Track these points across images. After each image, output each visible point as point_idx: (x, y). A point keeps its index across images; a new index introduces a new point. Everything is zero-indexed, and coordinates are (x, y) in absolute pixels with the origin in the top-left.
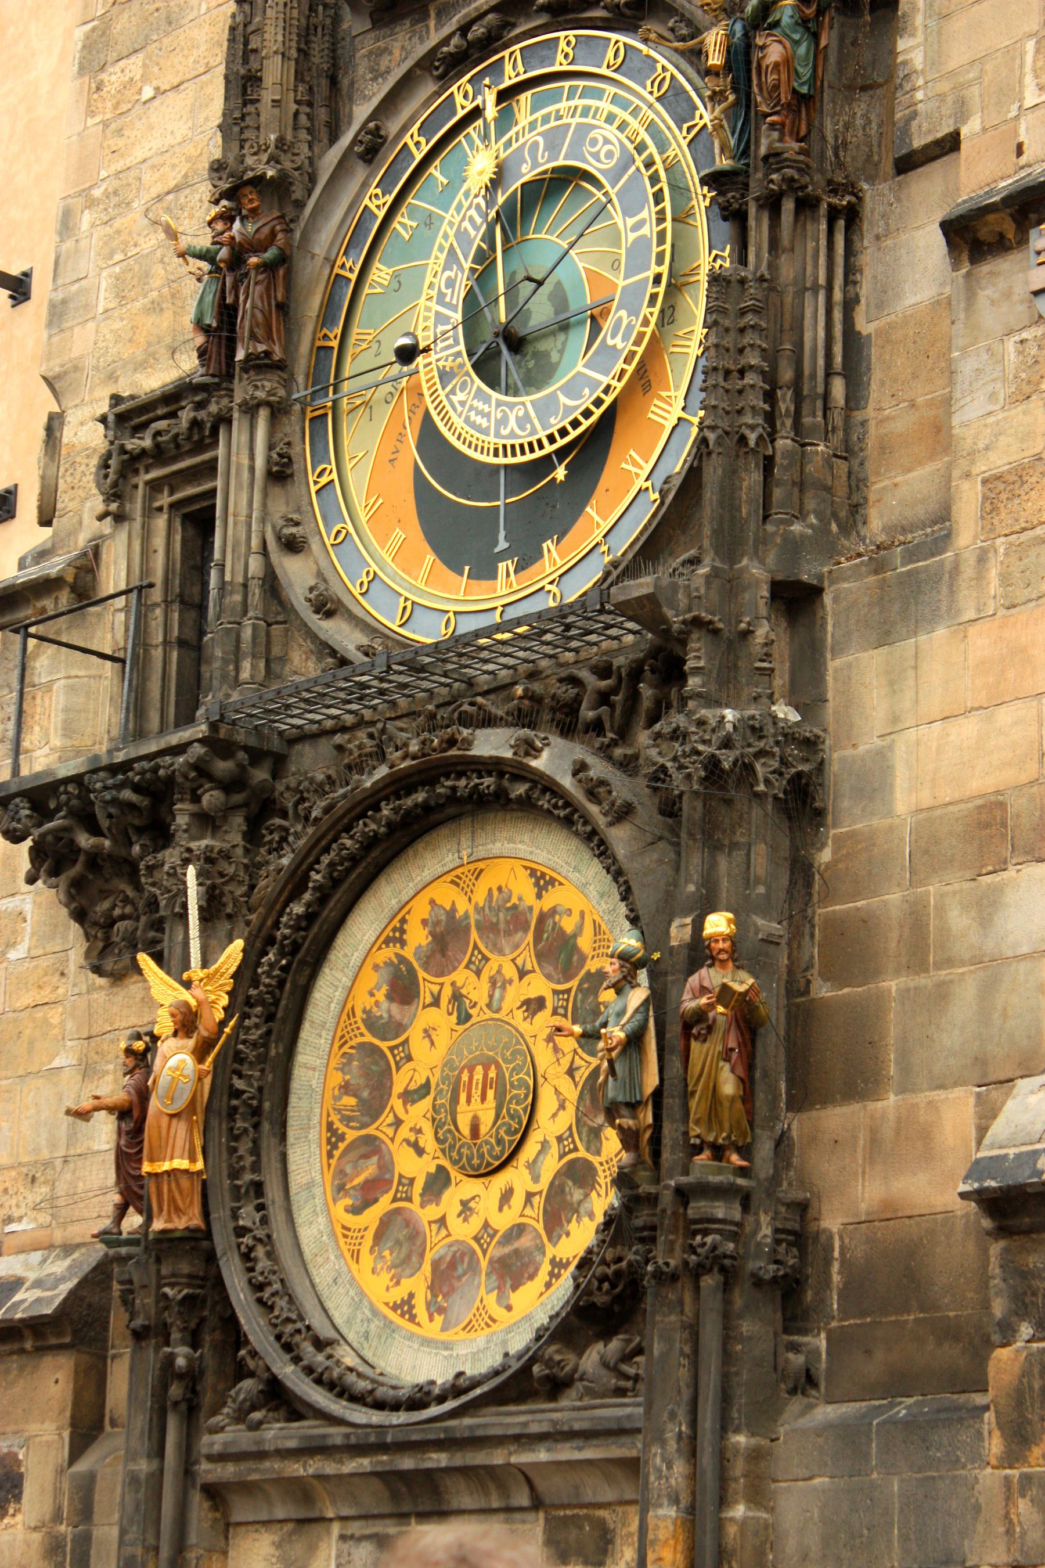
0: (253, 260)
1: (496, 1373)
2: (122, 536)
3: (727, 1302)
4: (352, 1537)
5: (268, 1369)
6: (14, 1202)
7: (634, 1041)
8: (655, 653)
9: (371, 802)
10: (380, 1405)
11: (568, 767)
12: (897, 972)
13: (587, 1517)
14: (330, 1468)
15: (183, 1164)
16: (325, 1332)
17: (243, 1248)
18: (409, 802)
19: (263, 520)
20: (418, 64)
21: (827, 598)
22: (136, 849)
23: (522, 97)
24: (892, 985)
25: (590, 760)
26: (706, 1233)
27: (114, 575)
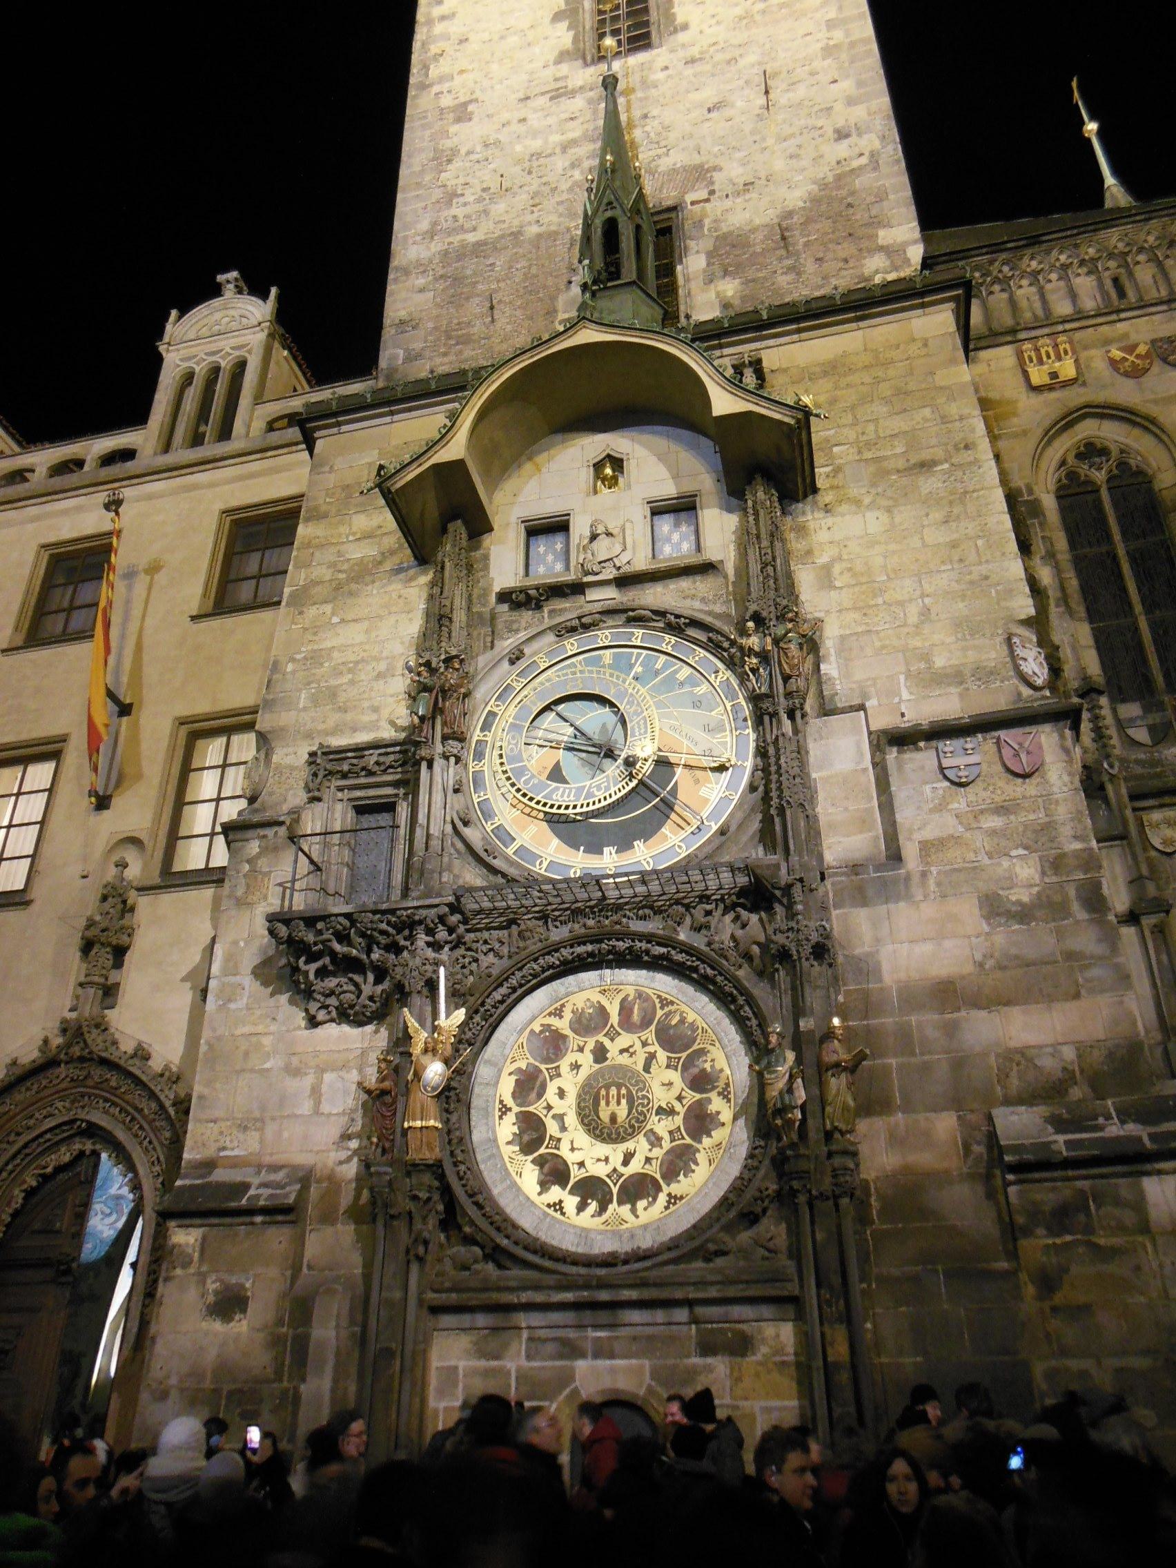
1: (669, 1249)
2: (318, 807)
4: (539, 1339)
5: (492, 1240)
6: (228, 1139)
8: (743, 892)
10: (575, 1263)
12: (895, 1056)
13: (729, 1329)
17: (462, 1173)
18: (580, 950)
19: (452, 808)
20: (549, 628)
22: (375, 956)
23: (608, 652)
24: (893, 1062)
26: (843, 1175)
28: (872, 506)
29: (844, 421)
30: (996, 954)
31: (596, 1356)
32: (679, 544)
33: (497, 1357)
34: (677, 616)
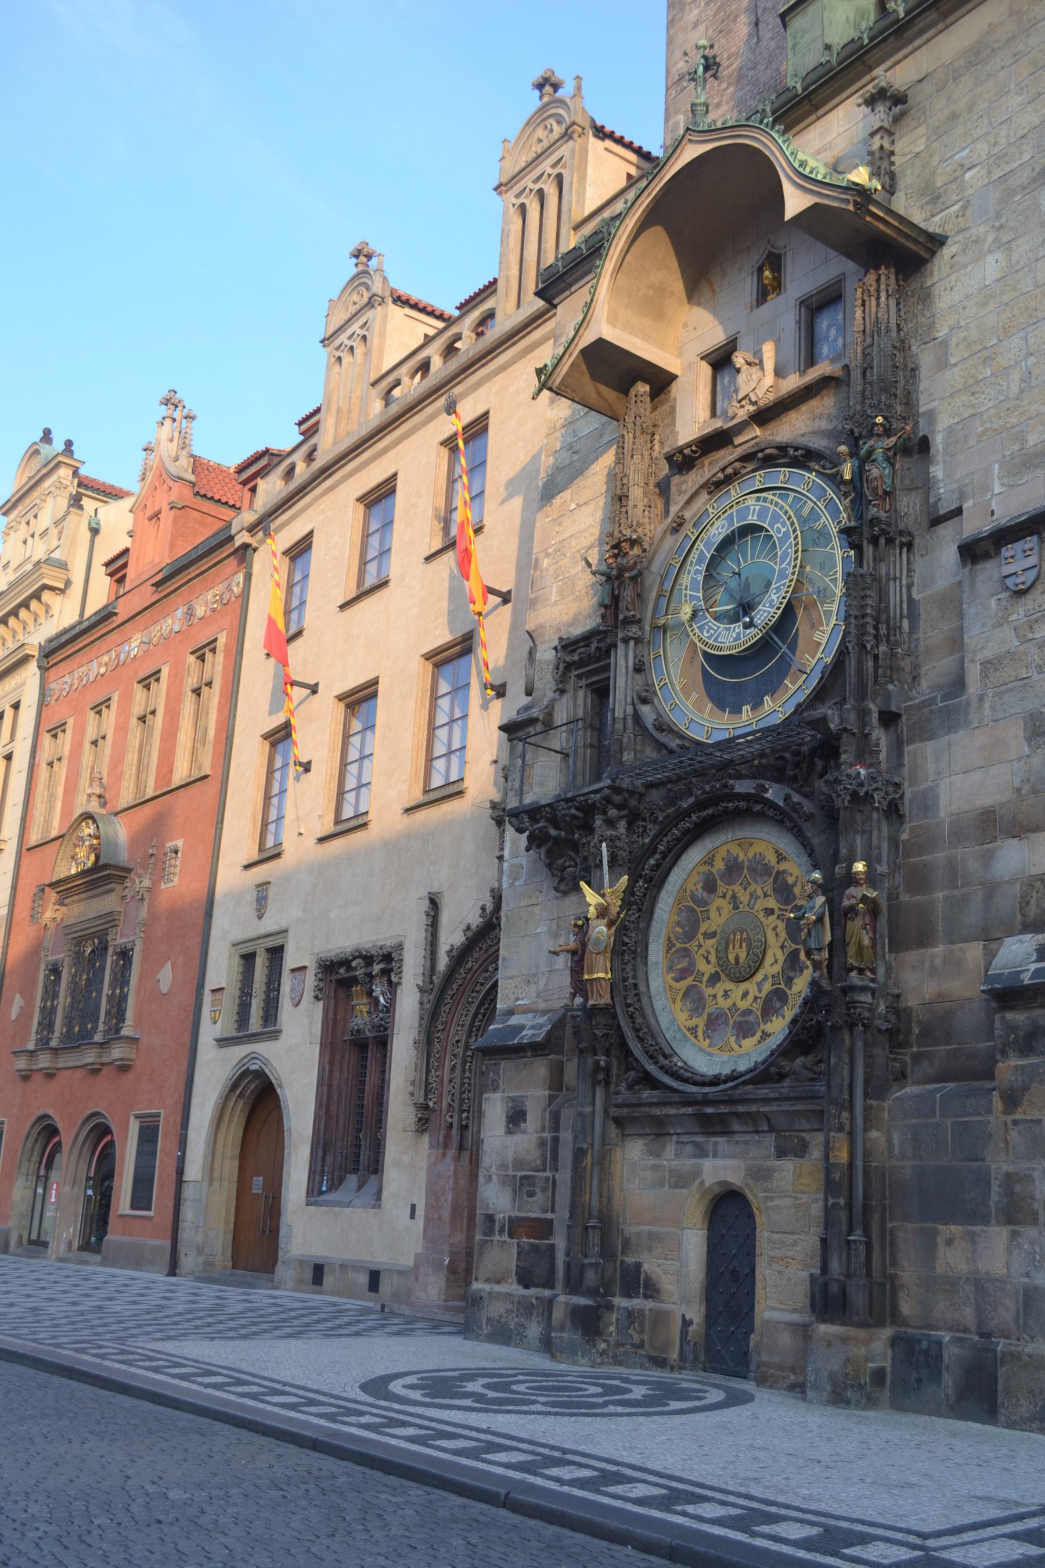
0: (627, 575)
2: (565, 698)
3: (865, 1040)
7: (820, 920)
9: (686, 814)
10: (696, 1084)
11: (782, 796)
14: (672, 1111)
15: (601, 975)
16: (668, 1051)
18: (704, 814)
19: (632, 689)
21: (904, 719)
24: (940, 895)
25: (792, 793)
27: (561, 716)
28: (998, 244)
29: (979, 132)
30: (1033, 779)
31: (715, 1156)
32: (835, 340)
33: (659, 1156)
34: (796, 449)
